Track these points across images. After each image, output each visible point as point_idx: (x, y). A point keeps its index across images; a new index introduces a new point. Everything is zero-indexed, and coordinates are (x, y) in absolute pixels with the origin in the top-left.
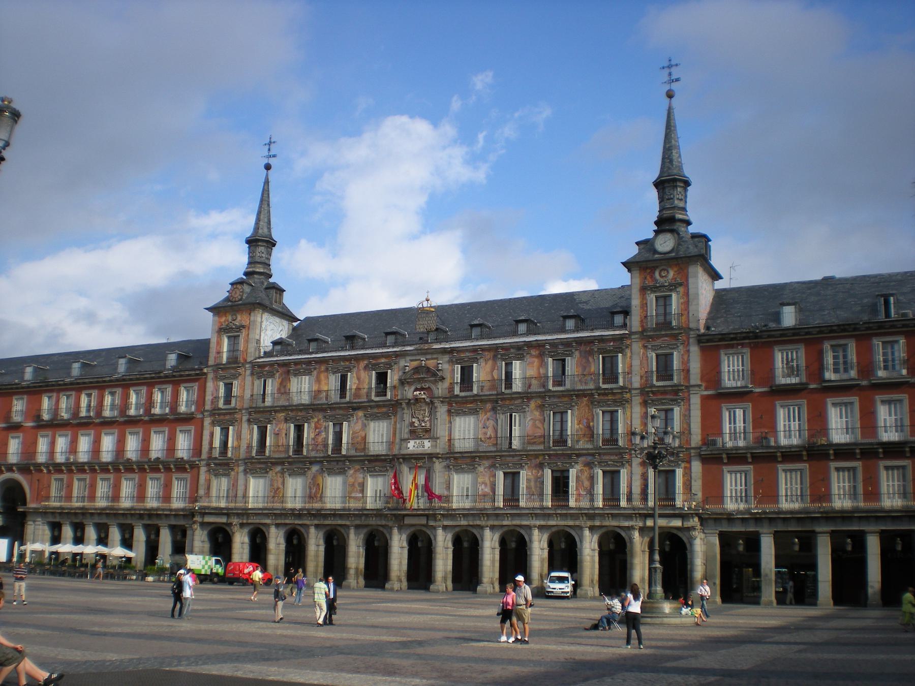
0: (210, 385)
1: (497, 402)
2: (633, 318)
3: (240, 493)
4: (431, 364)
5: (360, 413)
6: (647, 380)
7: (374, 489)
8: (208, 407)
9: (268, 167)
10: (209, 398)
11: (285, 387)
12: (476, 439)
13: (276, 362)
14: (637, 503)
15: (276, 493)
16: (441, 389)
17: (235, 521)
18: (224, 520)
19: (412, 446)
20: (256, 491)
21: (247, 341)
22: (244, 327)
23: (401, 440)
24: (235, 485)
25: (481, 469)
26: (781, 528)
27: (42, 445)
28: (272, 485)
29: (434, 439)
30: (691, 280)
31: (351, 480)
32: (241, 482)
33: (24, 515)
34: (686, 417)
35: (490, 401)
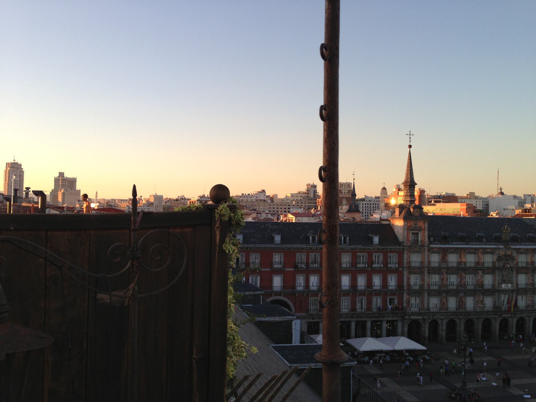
0: (405, 256)
1: (534, 270)
7: (489, 302)
9: (410, 146)
10: (405, 261)
11: (444, 259)
12: (526, 284)
13: (441, 248)
18: (421, 317)
22: (422, 229)
23: (498, 283)
24: (422, 302)
28: (441, 301)
29: (511, 283)
31: (477, 299)
32: (426, 300)
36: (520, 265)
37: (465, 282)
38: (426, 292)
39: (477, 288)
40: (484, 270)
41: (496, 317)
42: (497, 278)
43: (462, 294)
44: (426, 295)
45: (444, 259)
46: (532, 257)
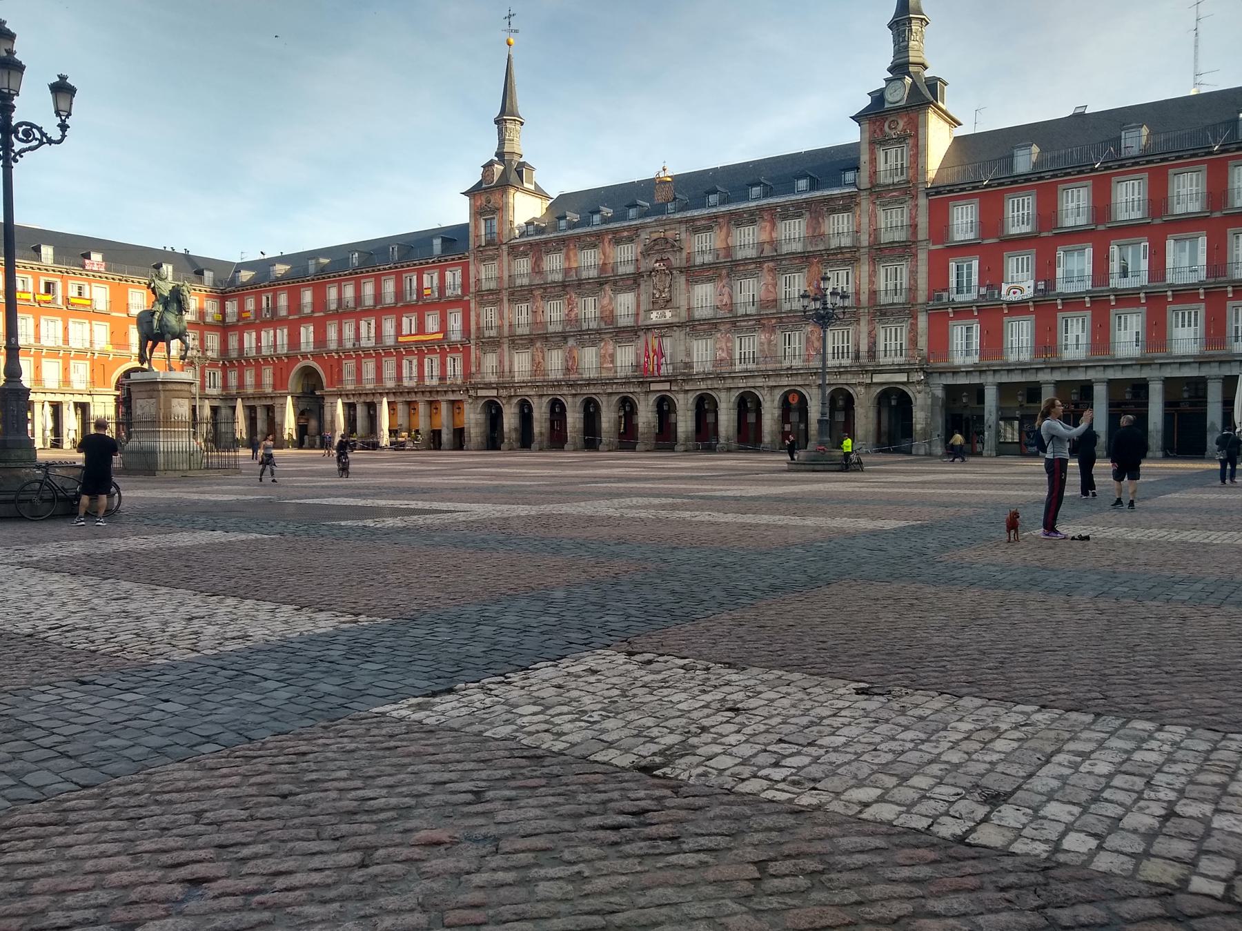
0: (472, 268)
2: (862, 174)
3: (507, 369)
4: (670, 234)
5: (607, 287)
6: (876, 238)
8: (472, 289)
10: (472, 280)
14: (864, 361)
15: (537, 367)
16: (677, 260)
17: (504, 393)
18: (494, 393)
19: (655, 317)
20: (521, 364)
21: (501, 223)
24: (501, 362)
25: (719, 335)
26: (1005, 379)
27: (332, 333)
28: (533, 360)
30: (920, 131)
32: (506, 359)
33: (322, 397)
34: (913, 274)
35: (725, 267)
36: (699, 260)
37: (576, 315)
38: (506, 340)
39: (603, 325)
40: (615, 283)
41: (638, 390)
42: (642, 298)
43: (571, 342)
44: (506, 347)
45: (537, 270)
46: (728, 235)
